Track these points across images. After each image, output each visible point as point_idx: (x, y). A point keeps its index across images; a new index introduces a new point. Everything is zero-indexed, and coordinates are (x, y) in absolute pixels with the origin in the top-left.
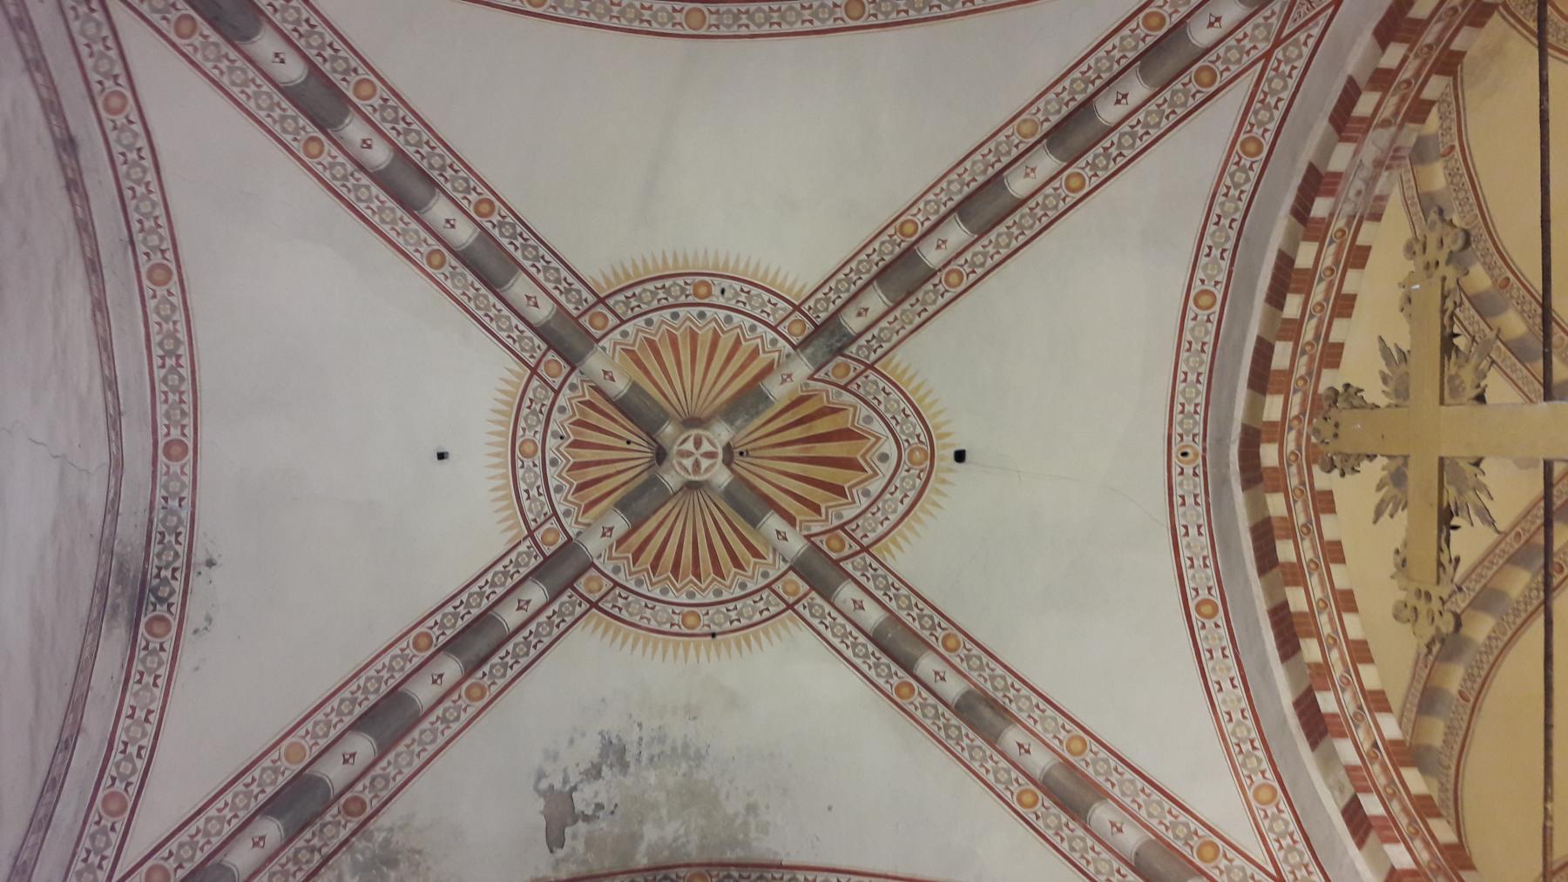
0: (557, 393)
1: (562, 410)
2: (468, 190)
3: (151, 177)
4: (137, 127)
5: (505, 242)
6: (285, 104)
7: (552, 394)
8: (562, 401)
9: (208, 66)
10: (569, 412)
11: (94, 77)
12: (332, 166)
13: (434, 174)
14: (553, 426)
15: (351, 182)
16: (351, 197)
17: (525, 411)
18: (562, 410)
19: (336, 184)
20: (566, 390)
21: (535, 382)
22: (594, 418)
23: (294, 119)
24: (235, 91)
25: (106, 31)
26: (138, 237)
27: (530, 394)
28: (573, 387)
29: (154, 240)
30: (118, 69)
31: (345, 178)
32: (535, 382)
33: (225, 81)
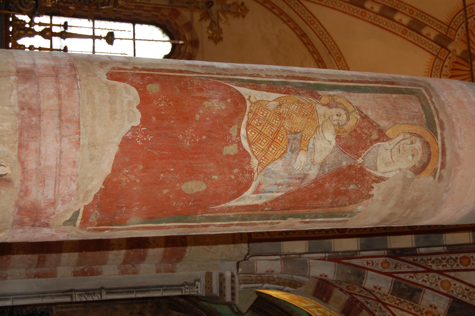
0: (444, 61)
1: (446, 66)
2: (405, 9)
3: (328, 36)
4: (320, 26)
5: (420, 19)
6: (352, 6)
7: (442, 62)
8: (446, 63)
9: (330, 5)
10: (449, 66)
11: (305, 19)
12: (370, 17)
13: (396, 8)
14: (443, 72)
15: (377, 19)
16: (378, 23)
17: (434, 70)
18: (446, 66)
19: (373, 21)
20: (448, 60)
21: (437, 60)
22: (457, 66)
23: (356, 9)
24: (339, 8)
25: (303, 8)
26: (331, 51)
27: (435, 64)
28: (450, 58)
29: (335, 51)
30: (310, 15)
31: (375, 19)
32: (437, 60)
33: (336, 7)
